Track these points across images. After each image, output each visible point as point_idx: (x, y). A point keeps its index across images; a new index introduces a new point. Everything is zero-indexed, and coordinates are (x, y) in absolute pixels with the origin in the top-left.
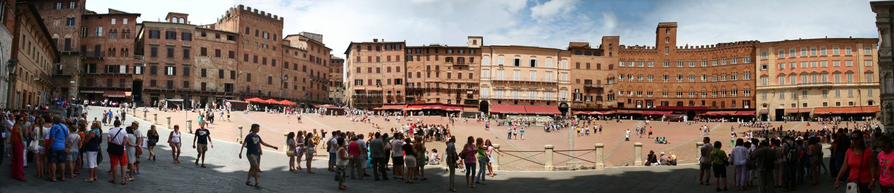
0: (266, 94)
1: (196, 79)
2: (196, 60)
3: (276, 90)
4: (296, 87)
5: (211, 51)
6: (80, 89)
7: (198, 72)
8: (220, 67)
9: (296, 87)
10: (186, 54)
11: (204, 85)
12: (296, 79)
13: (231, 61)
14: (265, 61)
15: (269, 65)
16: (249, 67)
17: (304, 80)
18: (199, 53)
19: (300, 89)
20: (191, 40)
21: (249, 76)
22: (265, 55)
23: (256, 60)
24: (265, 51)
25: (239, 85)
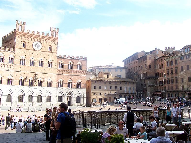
1: (180, 84)
5: (185, 67)
6: (151, 93)
8: (189, 75)
10: (176, 72)
18: (180, 70)
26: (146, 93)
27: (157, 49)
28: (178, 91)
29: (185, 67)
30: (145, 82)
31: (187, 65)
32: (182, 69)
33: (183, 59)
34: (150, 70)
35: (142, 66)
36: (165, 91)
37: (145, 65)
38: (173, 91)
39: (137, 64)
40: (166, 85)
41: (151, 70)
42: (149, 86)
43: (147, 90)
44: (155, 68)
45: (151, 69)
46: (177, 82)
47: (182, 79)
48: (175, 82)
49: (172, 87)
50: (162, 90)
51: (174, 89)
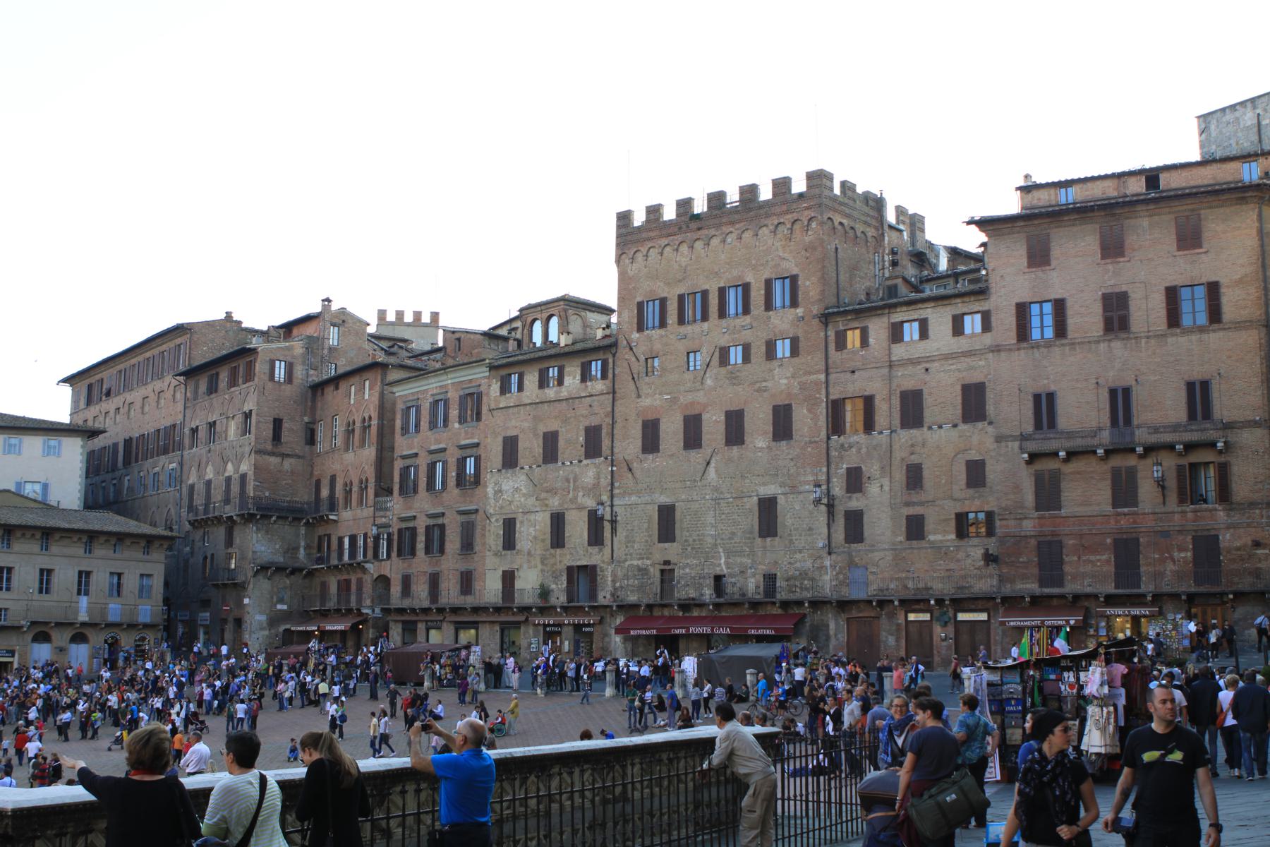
0: (753, 585)
1: (491, 561)
2: (490, 490)
3: (804, 562)
4: (915, 528)
5: (530, 447)
6: (274, 621)
7: (492, 535)
8: (555, 503)
9: (915, 528)
11: (509, 578)
12: (914, 476)
13: (591, 472)
14: (735, 429)
15: (759, 437)
16: (668, 474)
17: (976, 474)
19: (941, 534)
20: (478, 416)
21: (667, 515)
22: (733, 397)
23: (693, 435)
24: (734, 378)
25: (626, 565)
26: (239, 622)
27: (335, 307)
28: (476, 610)
29: (530, 447)
30: (237, 541)
31: (542, 429)
32: (510, 458)
33: (521, 388)
34: (272, 454)
35: (212, 425)
36: (377, 610)
37: (240, 418)
38: (441, 610)
39: (180, 406)
40: (393, 568)
41: (284, 456)
42: (263, 569)
43: (246, 601)
44: (311, 439)
45: (283, 450)
46: (467, 546)
47: (509, 526)
48: (453, 542)
49: (434, 581)
50: (359, 600)
51: (450, 593)
